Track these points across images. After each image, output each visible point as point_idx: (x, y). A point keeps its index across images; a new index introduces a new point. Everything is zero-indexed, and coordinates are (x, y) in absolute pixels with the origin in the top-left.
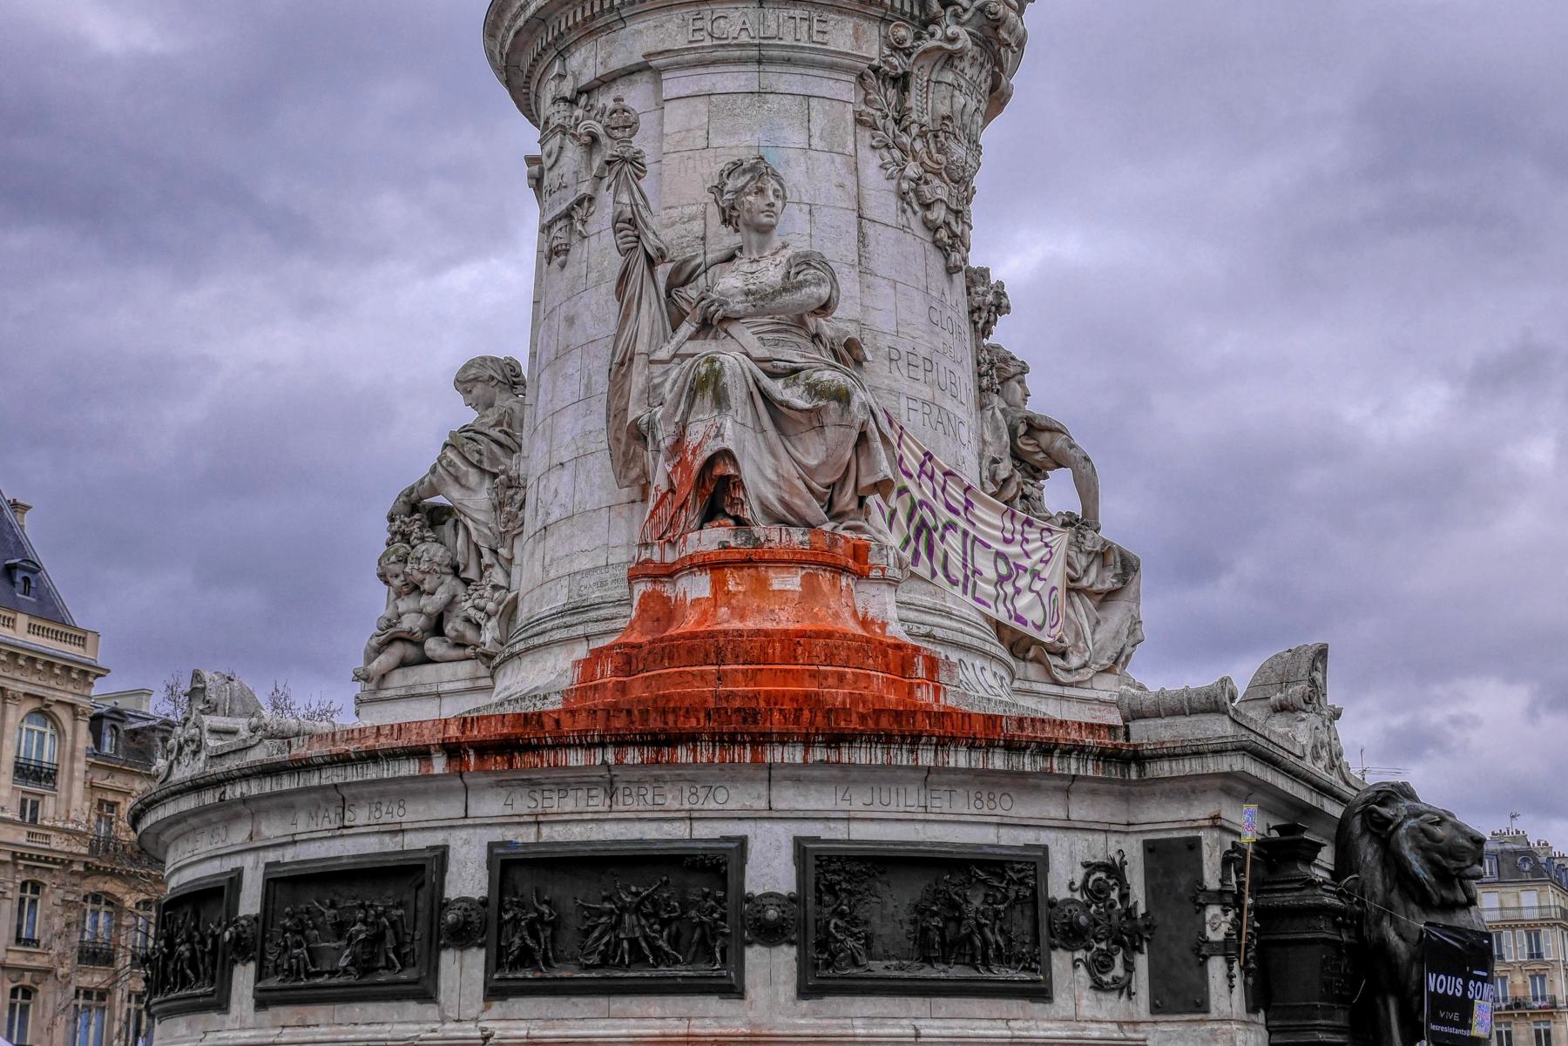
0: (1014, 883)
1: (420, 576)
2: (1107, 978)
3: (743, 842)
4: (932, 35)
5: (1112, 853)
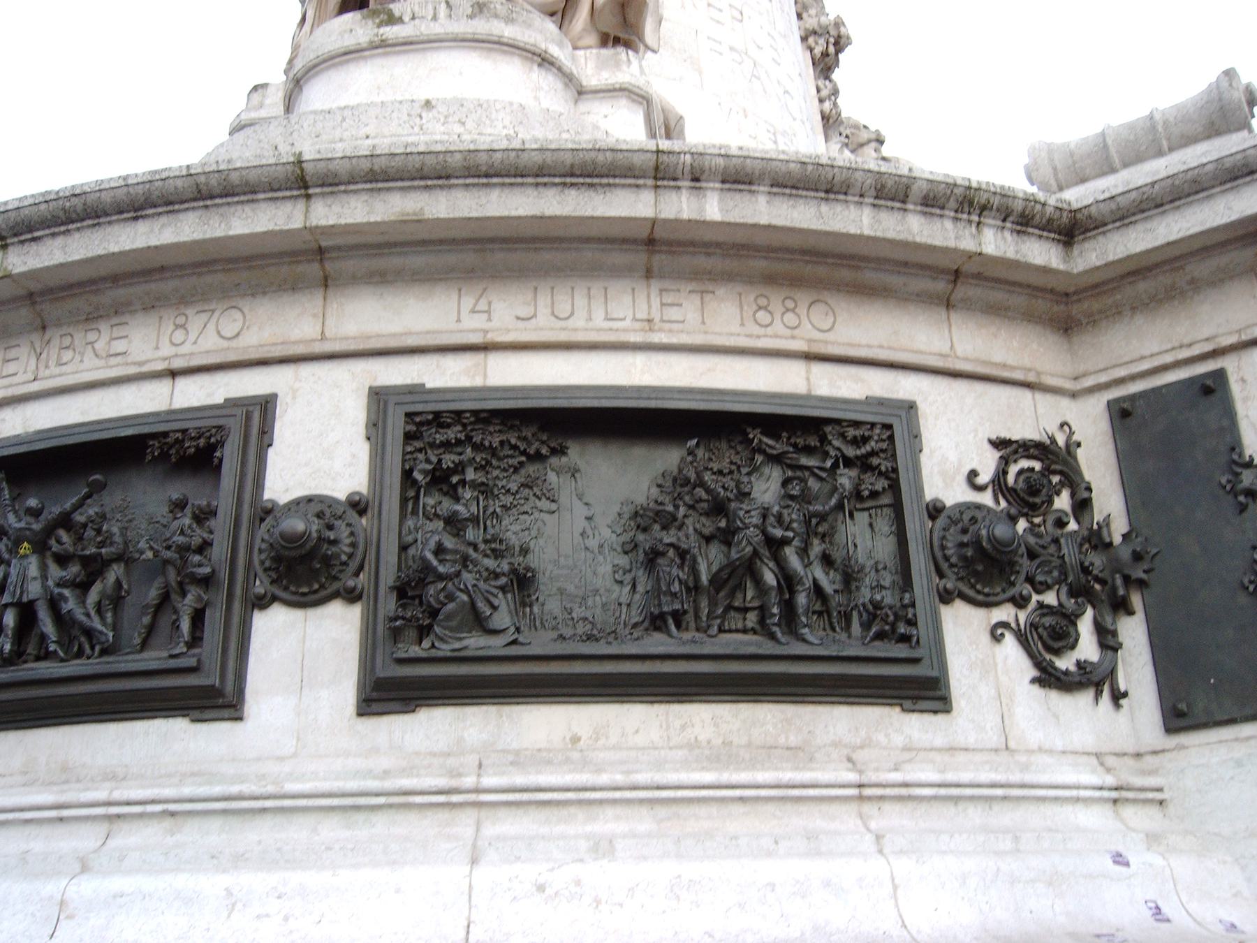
0: (848, 463)
2: (1065, 663)
3: (266, 406)
5: (1053, 428)
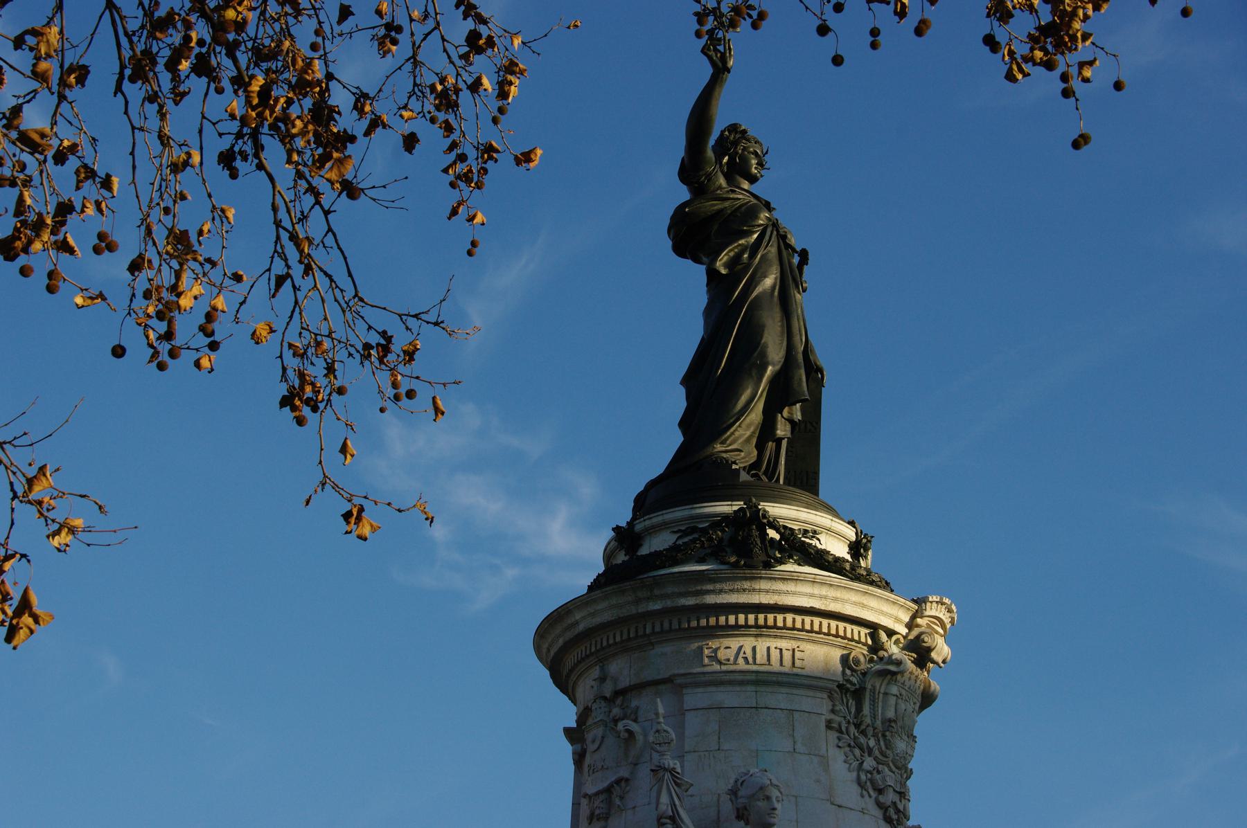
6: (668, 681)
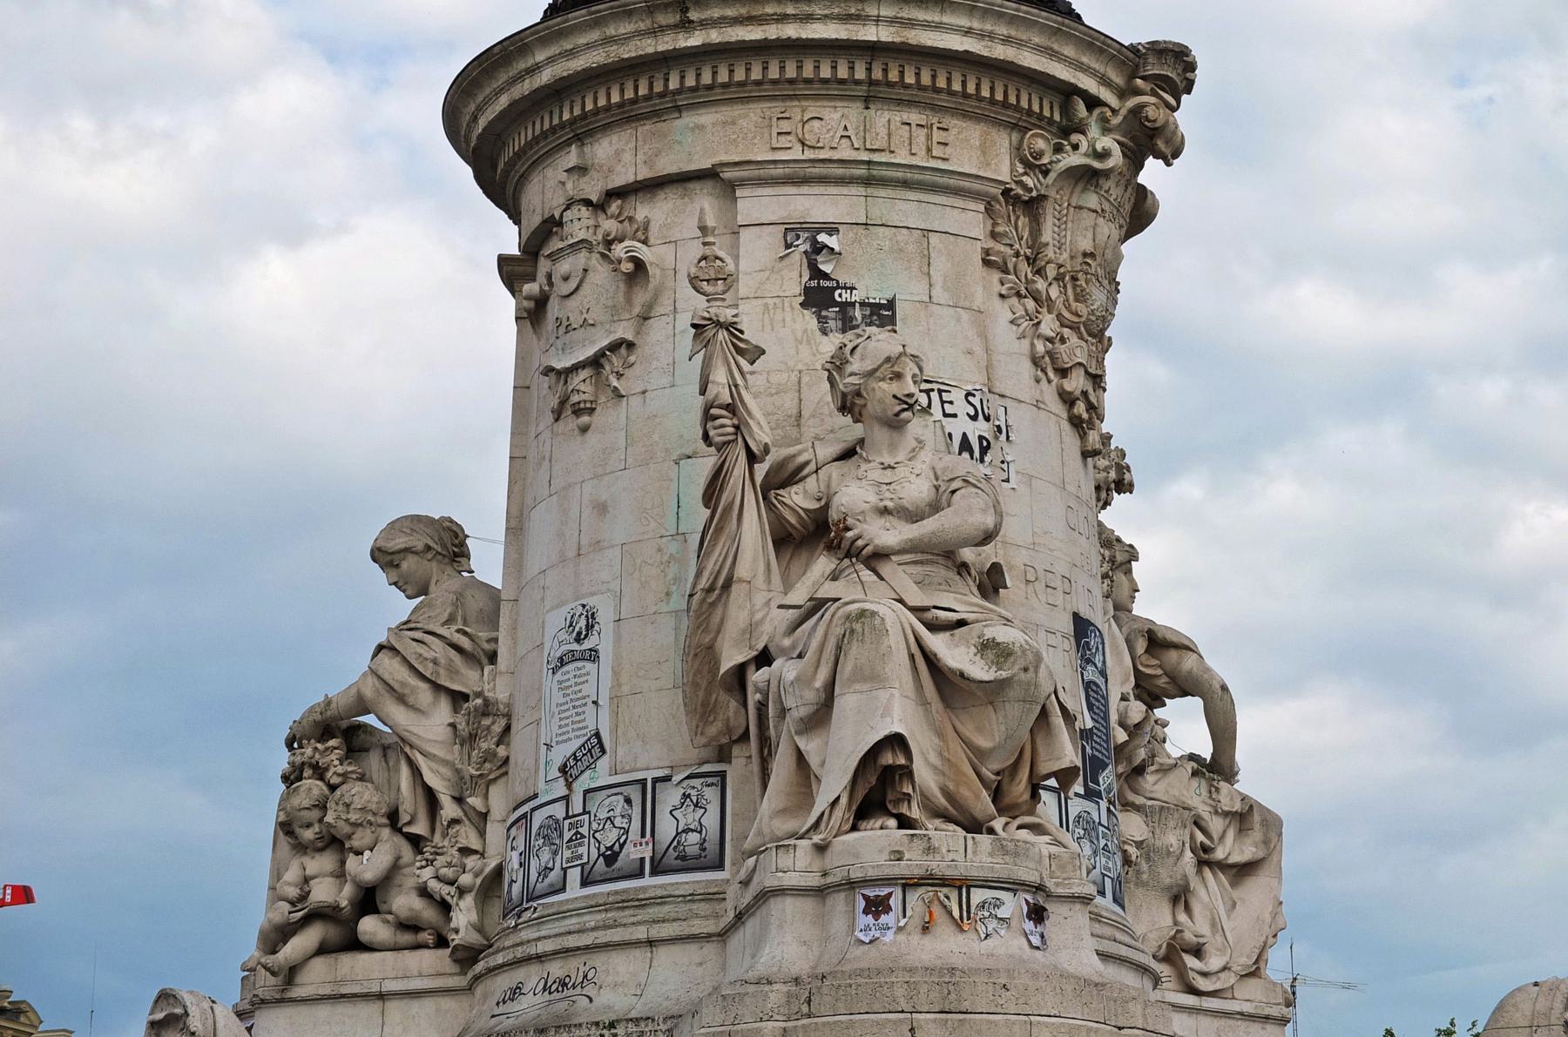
1: (347, 829)
4: (1075, 147)
6: (709, 175)
